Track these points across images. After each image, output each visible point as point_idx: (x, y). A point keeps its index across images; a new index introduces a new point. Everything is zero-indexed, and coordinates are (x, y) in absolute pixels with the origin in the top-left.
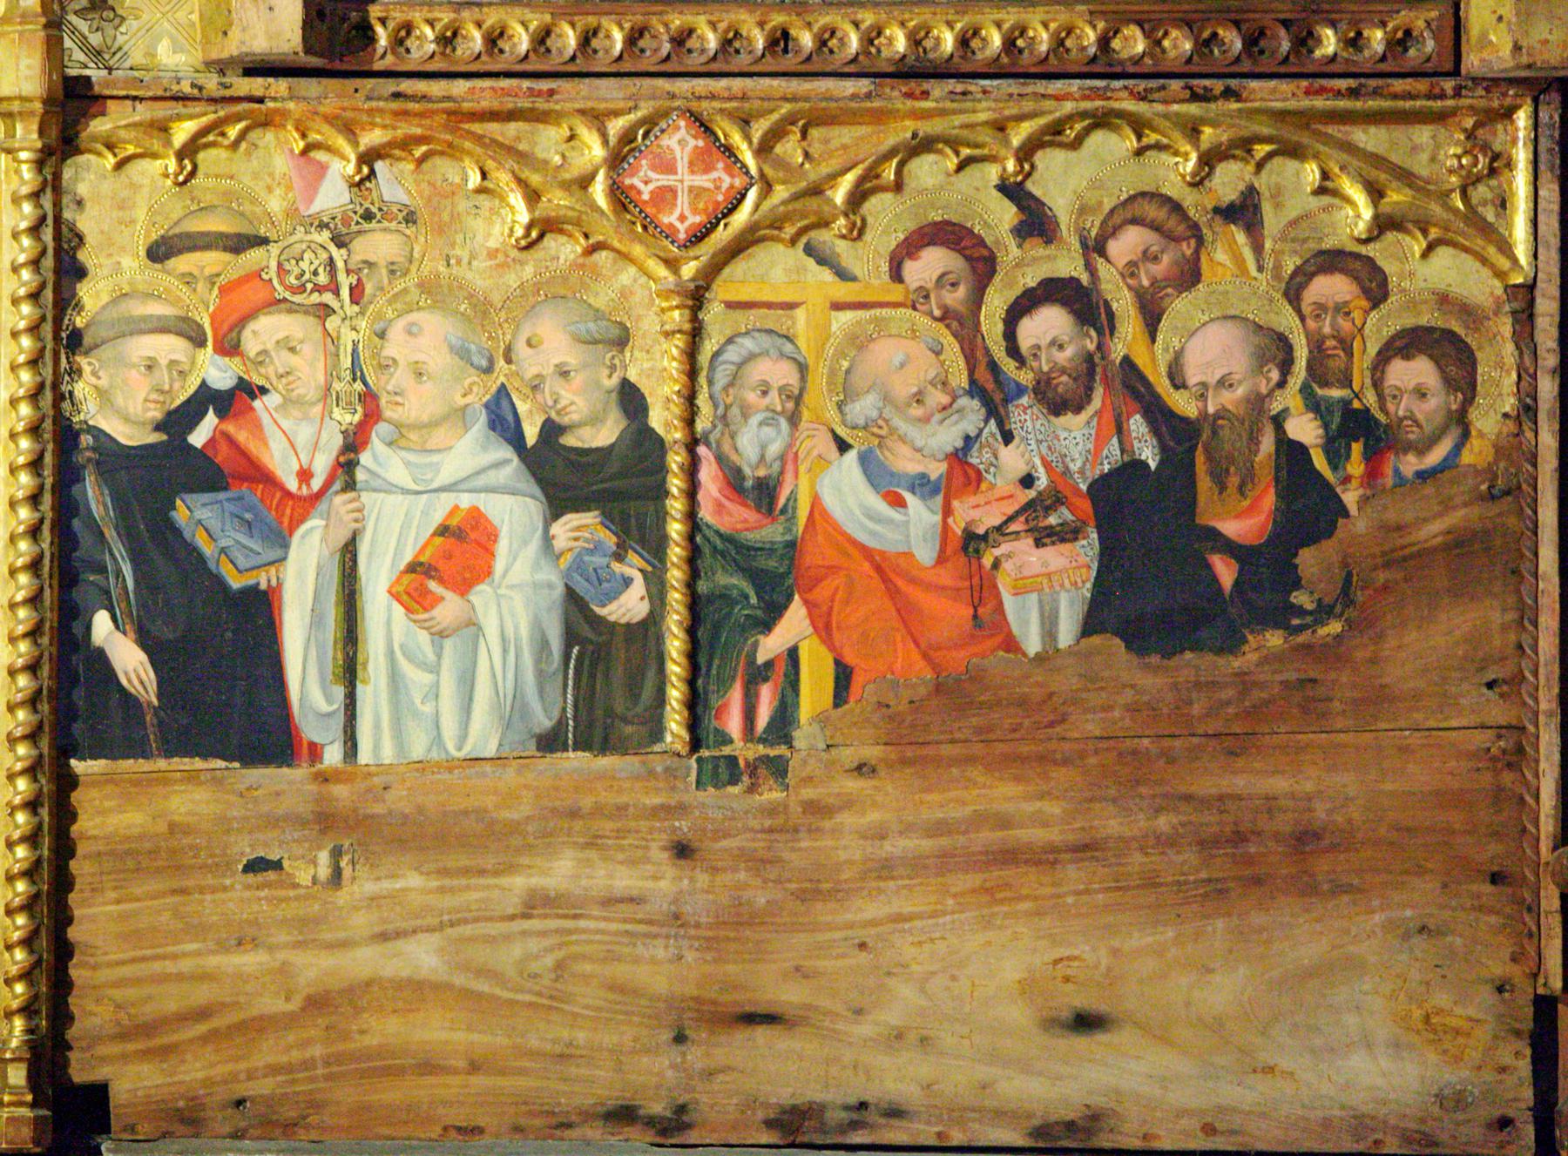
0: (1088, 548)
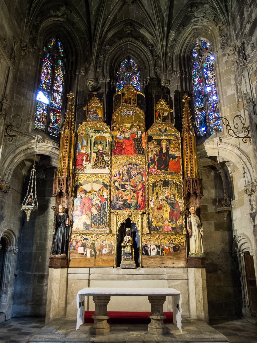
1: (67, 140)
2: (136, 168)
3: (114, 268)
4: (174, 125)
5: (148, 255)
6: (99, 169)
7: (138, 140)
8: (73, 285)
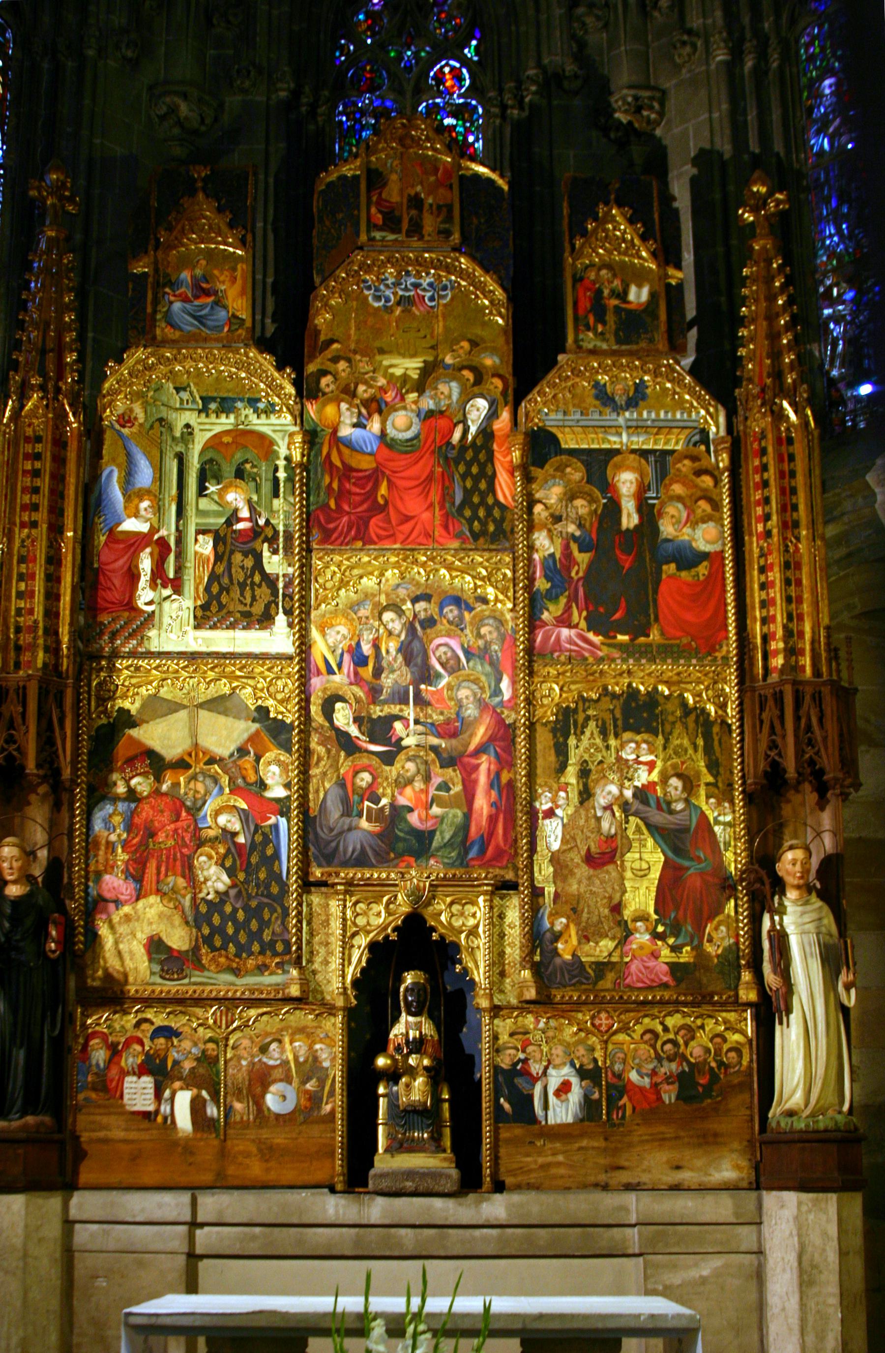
0: (676, 1085)
1: (38, 457)
2: (458, 624)
3: (333, 1190)
4: (688, 361)
5: (532, 1119)
6: (232, 626)
7: (469, 455)
8: (102, 1283)
